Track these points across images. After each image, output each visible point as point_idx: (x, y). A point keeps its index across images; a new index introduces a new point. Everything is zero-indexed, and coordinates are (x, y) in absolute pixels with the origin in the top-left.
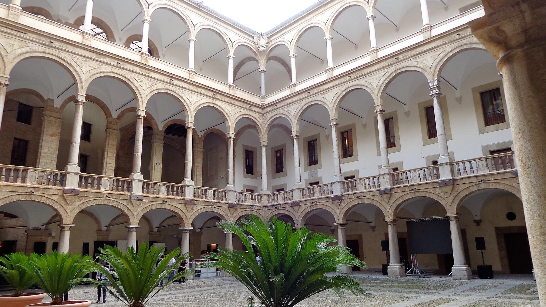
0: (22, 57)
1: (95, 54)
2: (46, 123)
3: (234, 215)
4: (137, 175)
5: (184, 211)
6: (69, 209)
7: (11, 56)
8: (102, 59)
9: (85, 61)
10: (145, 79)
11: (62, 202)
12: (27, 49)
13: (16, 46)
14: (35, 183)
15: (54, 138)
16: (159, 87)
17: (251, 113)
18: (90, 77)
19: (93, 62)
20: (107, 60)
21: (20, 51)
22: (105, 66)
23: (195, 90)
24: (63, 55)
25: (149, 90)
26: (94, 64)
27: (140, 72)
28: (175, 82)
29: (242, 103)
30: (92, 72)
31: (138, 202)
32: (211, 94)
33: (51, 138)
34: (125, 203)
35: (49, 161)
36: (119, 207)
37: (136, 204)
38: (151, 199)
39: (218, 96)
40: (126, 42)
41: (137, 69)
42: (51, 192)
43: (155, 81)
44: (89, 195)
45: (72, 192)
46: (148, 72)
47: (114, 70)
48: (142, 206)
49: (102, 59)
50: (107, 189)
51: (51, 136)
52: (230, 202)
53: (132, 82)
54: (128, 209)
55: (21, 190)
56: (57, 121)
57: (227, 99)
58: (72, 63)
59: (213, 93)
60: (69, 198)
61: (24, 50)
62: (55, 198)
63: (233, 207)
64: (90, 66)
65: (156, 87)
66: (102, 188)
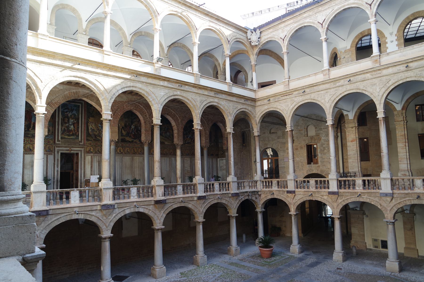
0: (294, 110)
1: (332, 83)
2: (347, 133)
4: (385, 174)
7: (289, 112)
8: (338, 84)
9: (327, 92)
10: (376, 81)
12: (295, 103)
13: (290, 105)
14: (314, 188)
15: (354, 143)
16: (394, 82)
18: (332, 103)
19: (332, 90)
20: (342, 82)
21: (292, 107)
22: (340, 88)
24: (313, 96)
25: (383, 90)
26: (332, 91)
27: (372, 77)
30: (333, 99)
31: (389, 199)
33: (352, 143)
34: (377, 199)
35: (354, 160)
36: (372, 203)
37: (387, 201)
40: (398, 31)
41: (368, 76)
42: (322, 193)
43: (388, 77)
44: (347, 194)
46: (380, 72)
47: (349, 87)
49: (338, 84)
50: (361, 188)
51: (352, 141)
53: (365, 91)
54: (381, 205)
56: (353, 129)
58: (319, 99)
60: (334, 197)
61: (293, 105)
62: (325, 197)
64: (330, 95)
65: (391, 83)
66: (357, 188)
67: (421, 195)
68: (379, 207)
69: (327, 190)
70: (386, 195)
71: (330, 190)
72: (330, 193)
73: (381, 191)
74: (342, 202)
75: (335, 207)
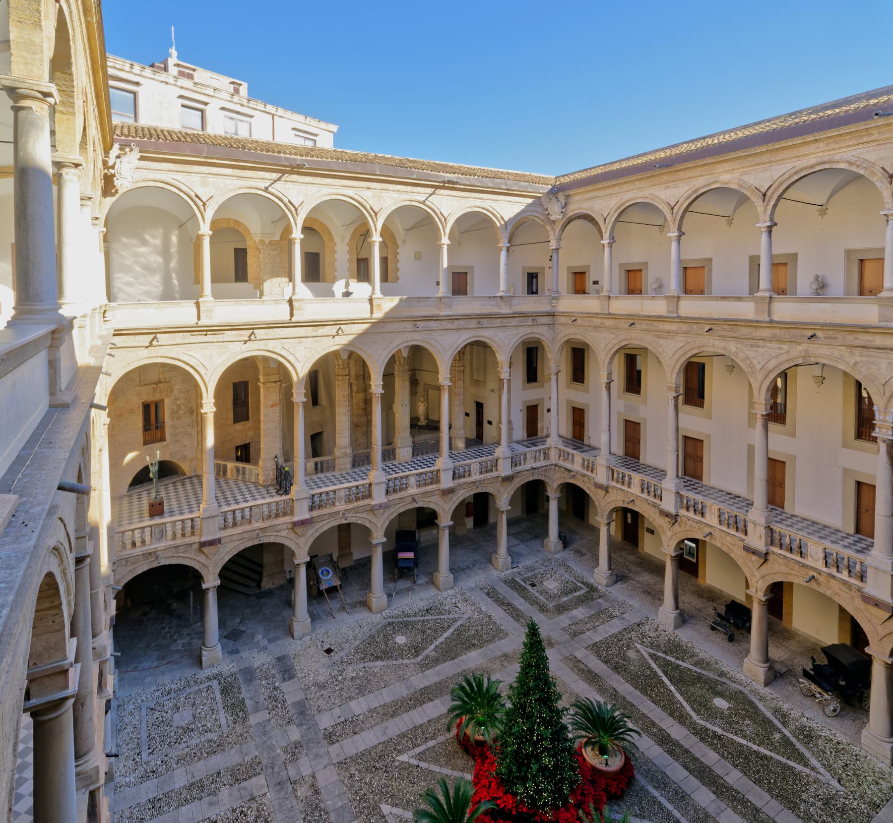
3: (509, 489)
5: (441, 503)
6: (301, 542)
11: (292, 535)
17: (535, 329)
23: (450, 326)
28: (421, 324)
29: (520, 319)
31: (381, 511)
32: (473, 323)
34: (365, 515)
36: (359, 522)
38: (397, 501)
39: (485, 322)
42: (279, 528)
45: (303, 523)
48: (386, 515)
52: (503, 474)
54: (370, 521)
55: (246, 535)
57: (498, 322)
59: (476, 321)
60: (299, 530)
62: (284, 533)
63: (507, 479)
67: (416, 497)
68: (368, 525)
69: (287, 519)
70: (380, 506)
71: (296, 519)
72: (295, 524)
73: (373, 503)
74: (313, 533)
75: (301, 545)
